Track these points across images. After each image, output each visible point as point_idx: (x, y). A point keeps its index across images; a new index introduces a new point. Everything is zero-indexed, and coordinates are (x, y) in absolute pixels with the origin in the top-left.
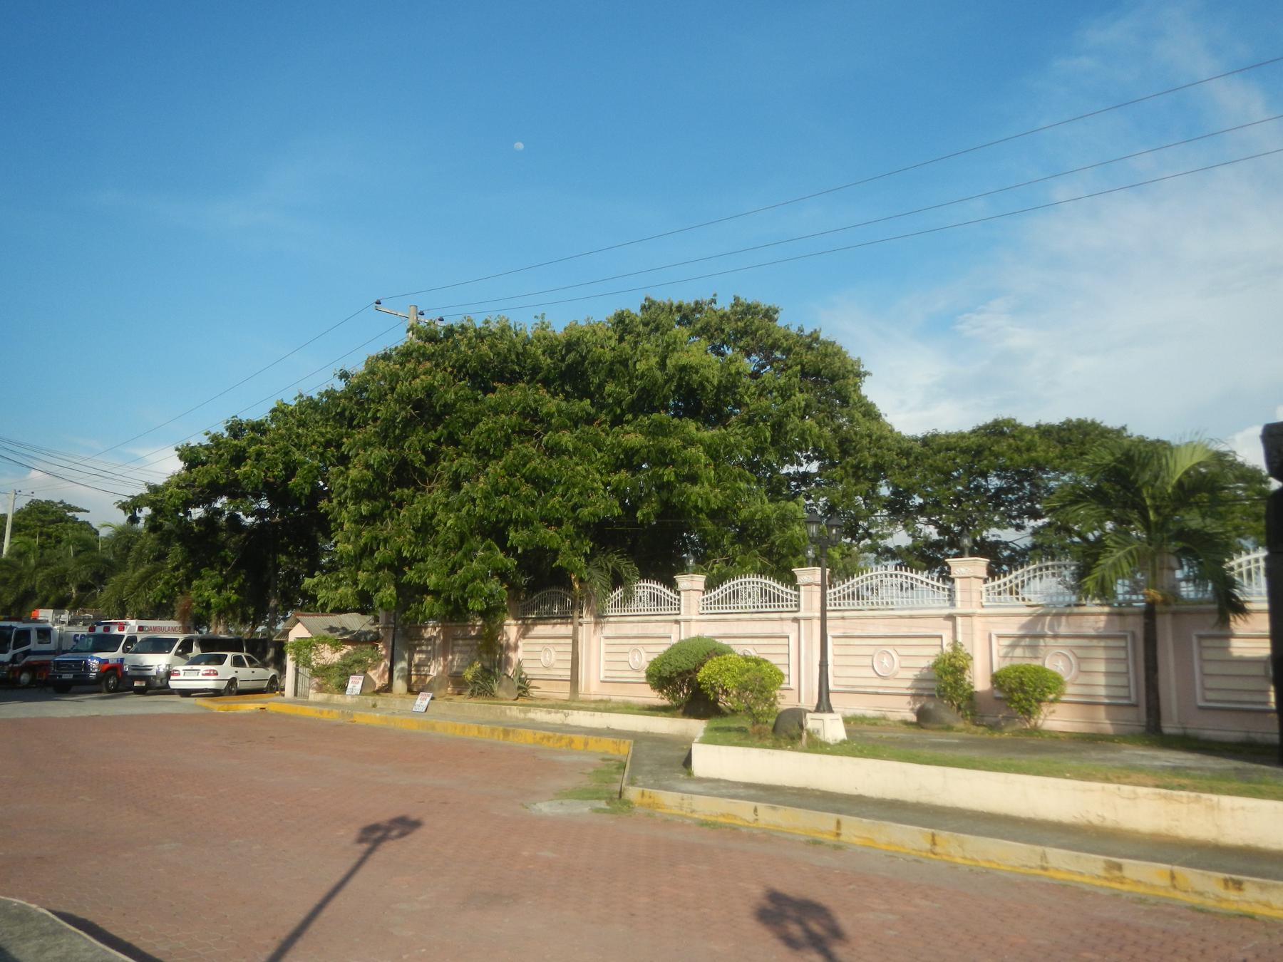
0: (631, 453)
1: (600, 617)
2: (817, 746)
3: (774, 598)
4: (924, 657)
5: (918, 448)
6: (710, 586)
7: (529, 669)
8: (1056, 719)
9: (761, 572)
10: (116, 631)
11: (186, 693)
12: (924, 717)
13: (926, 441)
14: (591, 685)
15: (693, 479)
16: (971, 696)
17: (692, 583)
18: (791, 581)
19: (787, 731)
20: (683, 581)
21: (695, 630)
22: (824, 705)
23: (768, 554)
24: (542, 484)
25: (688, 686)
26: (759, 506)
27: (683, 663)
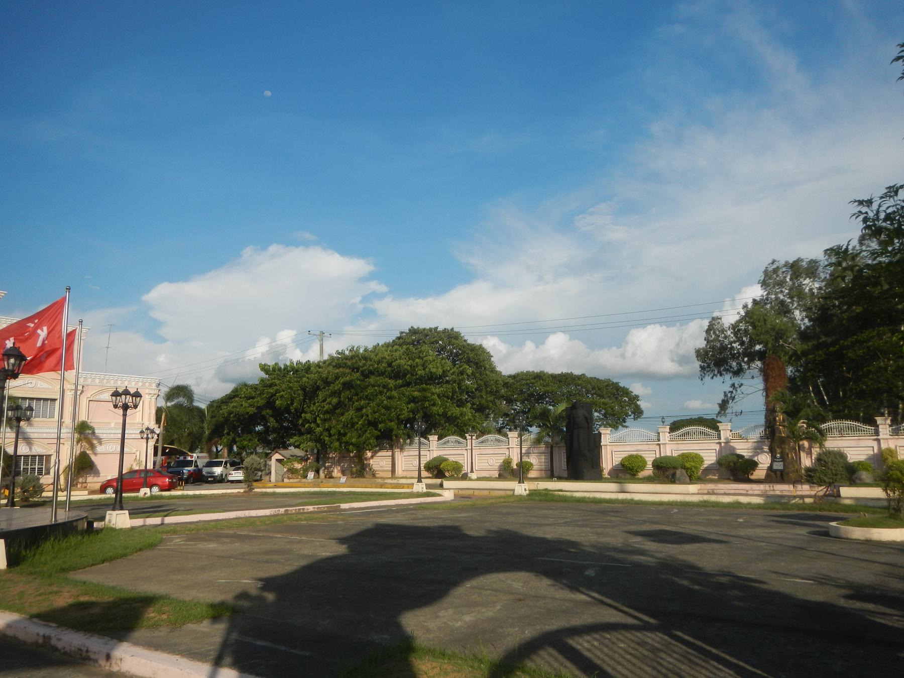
0: (414, 398)
1: (402, 449)
2: (470, 480)
3: (460, 443)
4: (500, 460)
5: (511, 381)
6: (439, 439)
7: (375, 467)
8: (532, 474)
9: (453, 435)
10: (189, 459)
11: (232, 482)
12: (500, 475)
13: (514, 377)
14: (399, 471)
15: (434, 405)
16: (513, 470)
17: (433, 438)
18: (465, 438)
19: (465, 477)
20: (431, 438)
21: (435, 454)
22: (472, 471)
23: (457, 426)
24: (387, 408)
25: (438, 470)
26: (455, 411)
27: (436, 463)
